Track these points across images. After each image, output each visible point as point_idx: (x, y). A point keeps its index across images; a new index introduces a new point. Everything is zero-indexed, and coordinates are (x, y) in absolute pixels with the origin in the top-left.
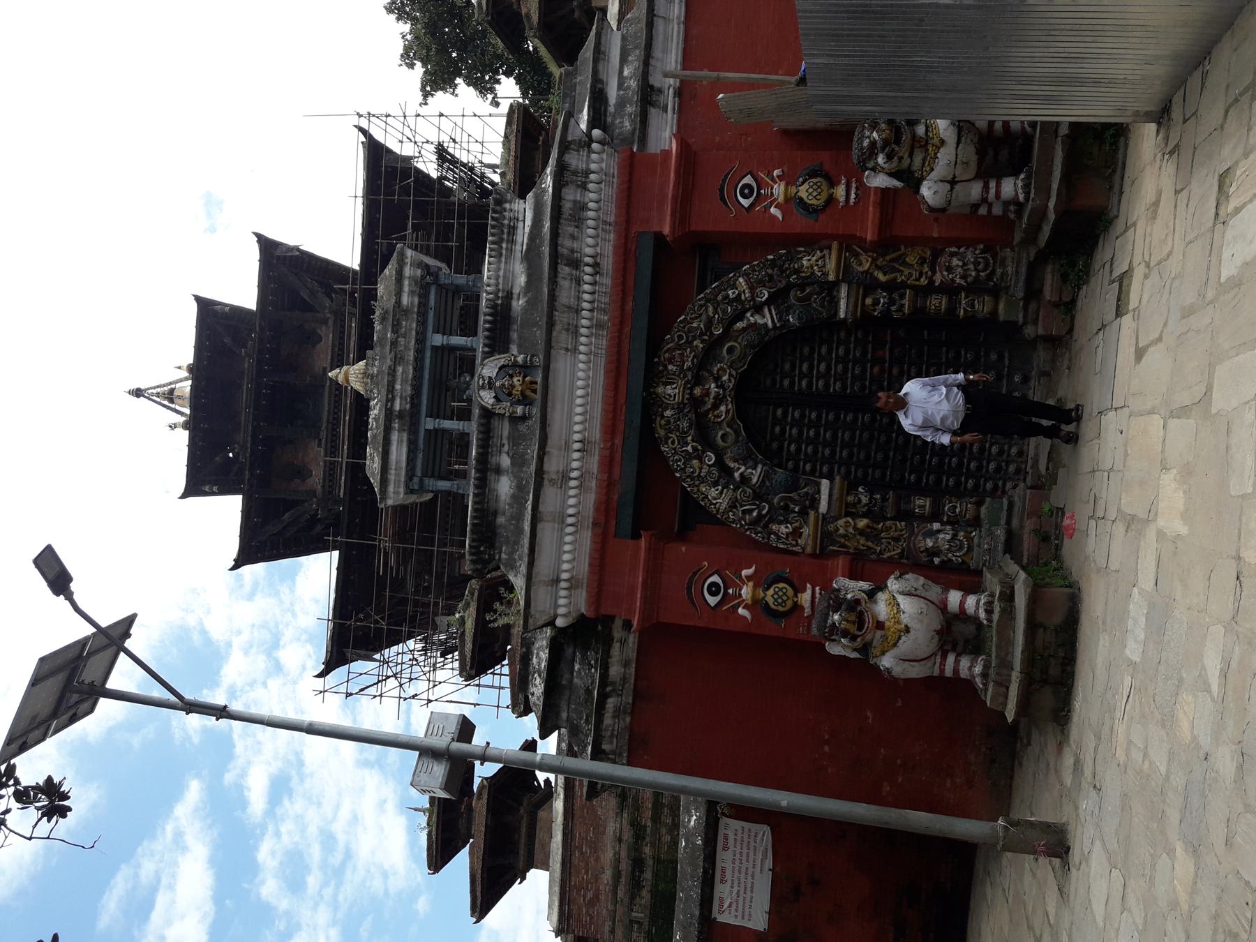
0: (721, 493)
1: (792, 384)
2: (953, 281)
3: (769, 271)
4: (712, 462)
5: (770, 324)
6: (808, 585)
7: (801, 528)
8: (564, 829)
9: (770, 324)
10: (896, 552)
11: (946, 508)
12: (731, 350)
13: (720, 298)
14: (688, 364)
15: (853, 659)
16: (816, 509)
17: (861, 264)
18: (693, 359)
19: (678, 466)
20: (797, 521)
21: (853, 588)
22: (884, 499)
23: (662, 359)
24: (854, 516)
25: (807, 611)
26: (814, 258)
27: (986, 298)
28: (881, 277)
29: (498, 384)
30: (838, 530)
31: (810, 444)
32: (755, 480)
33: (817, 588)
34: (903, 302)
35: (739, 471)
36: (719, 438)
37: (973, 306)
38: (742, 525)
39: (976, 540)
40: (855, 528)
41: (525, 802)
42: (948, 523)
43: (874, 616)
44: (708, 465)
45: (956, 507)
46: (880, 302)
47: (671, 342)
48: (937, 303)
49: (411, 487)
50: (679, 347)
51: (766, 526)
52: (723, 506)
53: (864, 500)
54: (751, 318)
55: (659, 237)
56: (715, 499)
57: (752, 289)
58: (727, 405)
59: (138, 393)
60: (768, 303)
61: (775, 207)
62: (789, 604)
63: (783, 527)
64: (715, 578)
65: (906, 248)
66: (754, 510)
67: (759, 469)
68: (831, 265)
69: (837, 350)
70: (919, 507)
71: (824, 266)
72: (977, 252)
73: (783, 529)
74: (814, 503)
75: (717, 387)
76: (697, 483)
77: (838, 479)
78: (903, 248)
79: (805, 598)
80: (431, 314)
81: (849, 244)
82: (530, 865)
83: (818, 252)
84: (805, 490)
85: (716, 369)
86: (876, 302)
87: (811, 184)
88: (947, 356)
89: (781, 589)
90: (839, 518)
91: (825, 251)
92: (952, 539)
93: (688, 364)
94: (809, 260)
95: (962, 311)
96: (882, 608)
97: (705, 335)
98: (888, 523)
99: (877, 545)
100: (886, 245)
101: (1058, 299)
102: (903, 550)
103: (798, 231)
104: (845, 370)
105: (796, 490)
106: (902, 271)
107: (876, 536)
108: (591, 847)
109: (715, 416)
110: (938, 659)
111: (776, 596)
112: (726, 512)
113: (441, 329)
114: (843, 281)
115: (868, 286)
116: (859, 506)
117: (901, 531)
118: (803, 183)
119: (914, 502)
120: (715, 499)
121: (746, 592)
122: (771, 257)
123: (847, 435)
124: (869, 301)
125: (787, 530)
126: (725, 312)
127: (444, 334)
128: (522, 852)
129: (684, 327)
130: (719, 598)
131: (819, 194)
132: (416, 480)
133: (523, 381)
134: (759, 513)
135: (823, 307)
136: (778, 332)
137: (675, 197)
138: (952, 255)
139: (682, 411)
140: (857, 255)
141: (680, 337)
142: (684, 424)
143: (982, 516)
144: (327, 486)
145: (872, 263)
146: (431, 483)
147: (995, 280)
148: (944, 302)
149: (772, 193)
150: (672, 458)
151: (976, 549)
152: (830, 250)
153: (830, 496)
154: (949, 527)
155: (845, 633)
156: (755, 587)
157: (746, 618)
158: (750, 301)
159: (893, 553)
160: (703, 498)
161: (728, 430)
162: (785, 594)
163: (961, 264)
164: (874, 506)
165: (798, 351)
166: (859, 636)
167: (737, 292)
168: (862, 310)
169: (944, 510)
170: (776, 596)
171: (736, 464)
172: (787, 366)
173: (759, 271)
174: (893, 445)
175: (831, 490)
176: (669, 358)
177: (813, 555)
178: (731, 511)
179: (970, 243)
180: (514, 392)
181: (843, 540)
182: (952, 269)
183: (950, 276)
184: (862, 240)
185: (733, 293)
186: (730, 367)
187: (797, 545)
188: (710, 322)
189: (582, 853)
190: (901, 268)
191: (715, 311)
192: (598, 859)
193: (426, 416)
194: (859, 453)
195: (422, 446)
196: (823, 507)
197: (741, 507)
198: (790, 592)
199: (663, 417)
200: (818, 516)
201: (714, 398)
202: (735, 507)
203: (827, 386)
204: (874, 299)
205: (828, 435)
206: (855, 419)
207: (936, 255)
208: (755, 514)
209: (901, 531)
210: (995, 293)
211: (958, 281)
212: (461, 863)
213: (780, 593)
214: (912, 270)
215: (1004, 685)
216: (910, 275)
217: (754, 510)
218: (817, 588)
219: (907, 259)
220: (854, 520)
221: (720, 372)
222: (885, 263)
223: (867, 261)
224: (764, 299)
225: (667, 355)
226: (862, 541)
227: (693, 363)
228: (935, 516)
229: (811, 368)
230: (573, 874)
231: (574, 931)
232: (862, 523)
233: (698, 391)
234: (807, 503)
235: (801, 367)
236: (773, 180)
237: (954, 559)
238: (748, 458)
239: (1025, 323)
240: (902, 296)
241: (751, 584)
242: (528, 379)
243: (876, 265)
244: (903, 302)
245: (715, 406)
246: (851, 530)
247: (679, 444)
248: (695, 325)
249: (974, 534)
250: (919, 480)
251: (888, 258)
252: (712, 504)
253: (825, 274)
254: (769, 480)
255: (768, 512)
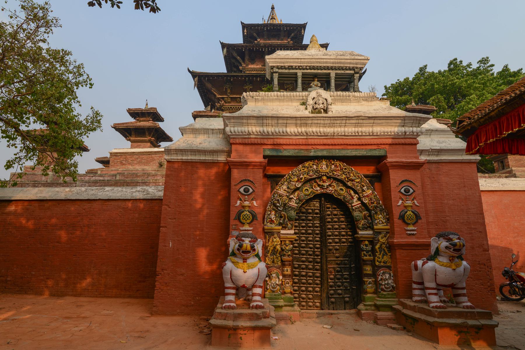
0: (285, 190)
1: (329, 215)
2: (379, 275)
3: (375, 203)
4: (297, 186)
5: (353, 205)
6: (252, 228)
7: (274, 223)
8: (145, 152)
9: (353, 205)
10: (268, 262)
11: (287, 280)
12: (342, 189)
13: (363, 183)
14: (335, 173)
15: (228, 250)
16: (282, 229)
17: (382, 238)
18: (337, 175)
19: (294, 172)
20: (277, 222)
21: (259, 247)
22: (289, 256)
23: (336, 163)
24: (281, 244)
25: (242, 228)
26: (382, 219)
27: (374, 289)
28: (377, 247)
29: (320, 98)
30: (275, 238)
31: (306, 224)
32: (290, 203)
33: (251, 232)
34: (368, 256)
35: (294, 196)
36: (306, 188)
37: (369, 284)
38: (272, 200)
39: (276, 294)
40: (277, 245)
41: (152, 139)
42: (282, 282)
43: (249, 258)
44: (295, 184)
45: (288, 284)
46: (367, 247)
47: (343, 166)
48: (368, 269)
49: (274, 68)
50: (342, 169)
51: (274, 209)
52: (279, 191)
53: (287, 248)
54: (355, 197)
55: (385, 157)
56: (282, 188)
57: (368, 196)
58: (320, 190)
59: (273, 8)
60: (363, 203)
61: (402, 202)
62: (244, 221)
63: (274, 216)
64: (251, 190)
65: (389, 255)
66: (279, 204)
67: (296, 205)
68: (380, 226)
69: (344, 232)
70: (287, 270)
71: (379, 224)
72: (392, 284)
73: (273, 217)
74: (284, 228)
75: (327, 186)
76: (288, 180)
77: (295, 236)
78: (390, 254)
79: (247, 227)
80: (342, 72)
81: (391, 232)
82: (132, 142)
83: (385, 221)
84: (289, 224)
85: (334, 184)
86: (366, 246)
87: (413, 216)
88: (345, 275)
89: (249, 217)
90: (280, 238)
91: (385, 223)
92: (277, 284)
93: (335, 173)
94: (381, 218)
95: (368, 280)
96: (252, 260)
97: (348, 179)
98: (279, 258)
99: (270, 254)
100: (391, 248)
101: (378, 319)
102: (268, 264)
103: (394, 212)
104: (336, 236)
105: (289, 220)
106: (380, 254)
107: (274, 253)
108: (140, 161)
109: (315, 186)
110: (232, 286)
111: (246, 215)
112: (277, 193)
113: (337, 77)
114: (374, 232)
115: (372, 242)
116: (285, 246)
117: (277, 263)
118: (412, 212)
119: (289, 267)
120: (282, 188)
121: (247, 203)
122: (381, 202)
123: (311, 239)
124: (367, 242)
125: (272, 217)
126: (357, 186)
127: (335, 78)
128: (136, 138)
129: (350, 170)
130: (244, 193)
131: (410, 219)
132: (277, 70)
133: (322, 108)
134: (278, 206)
135: (362, 225)
136: (350, 208)
137: (402, 162)
138: (390, 274)
139: (316, 172)
140: (385, 236)
141: (346, 169)
142: (311, 174)
143: (286, 295)
144: (249, 69)
145: (383, 242)
146: (276, 76)
147: (382, 292)
148: (369, 272)
149: (407, 200)
150: (296, 169)
151: (274, 294)
152: (386, 226)
153: (288, 234)
154: (280, 282)
155: (241, 246)
156: (249, 207)
157: (236, 203)
158: (363, 196)
159: (268, 261)
160: (282, 183)
161: (310, 191)
162: (248, 219)
163: (387, 278)
164: (285, 251)
165: (342, 216)
166: (239, 252)
167: (366, 190)
168: (362, 241)
169: (286, 279)
170: (246, 215)
171: (297, 195)
172: (335, 212)
173: (375, 198)
174: (308, 257)
175: (290, 234)
176: (337, 166)
177: (264, 229)
178: (278, 195)
179: (395, 281)
180: (317, 105)
181: (271, 240)
182: (384, 274)
183: (381, 274)
184: (393, 238)
185: (366, 189)
186: (335, 190)
187: (267, 222)
188: (352, 180)
189: (137, 158)
190: (381, 254)
191: (357, 182)
192: (137, 164)
193: (302, 73)
194: (304, 244)
195: (290, 72)
196: (283, 232)
197: (280, 199)
198: (248, 221)
199: (313, 164)
200: (280, 230)
201: (322, 185)
202: (280, 196)
203: (329, 229)
204: (368, 245)
205: (310, 231)
206: (317, 241)
207: (389, 267)
208: (278, 205)
209: (277, 263)
210: (375, 292)
211: (380, 277)
212: (130, 120)
213: (248, 217)
214: (382, 259)
215: (225, 317)
216: (379, 258)
217: (279, 204)
218: (251, 232)
219: (385, 256)
220: (280, 244)
221: (333, 186)
222: (383, 248)
223: (384, 241)
224: (364, 201)
225: (338, 164)
226: (272, 248)
227: (336, 175)
228: (284, 276)
229: (335, 222)
230: (130, 156)
231: (111, 158)
232: (278, 247)
233: (324, 178)
234: (284, 225)
235: (336, 218)
236: (413, 200)
237: (269, 286)
238: (299, 200)
239: (365, 305)
240: (370, 256)
241: (250, 205)
242: (322, 110)
243: (382, 244)
244: (368, 256)
245: (319, 185)
246: (275, 243)
247: (303, 172)
248: (352, 175)
249: (279, 293)
250: (296, 268)
251: (385, 248)
252: (280, 187)
253: (376, 224)
254: (291, 209)
255: (280, 210)
